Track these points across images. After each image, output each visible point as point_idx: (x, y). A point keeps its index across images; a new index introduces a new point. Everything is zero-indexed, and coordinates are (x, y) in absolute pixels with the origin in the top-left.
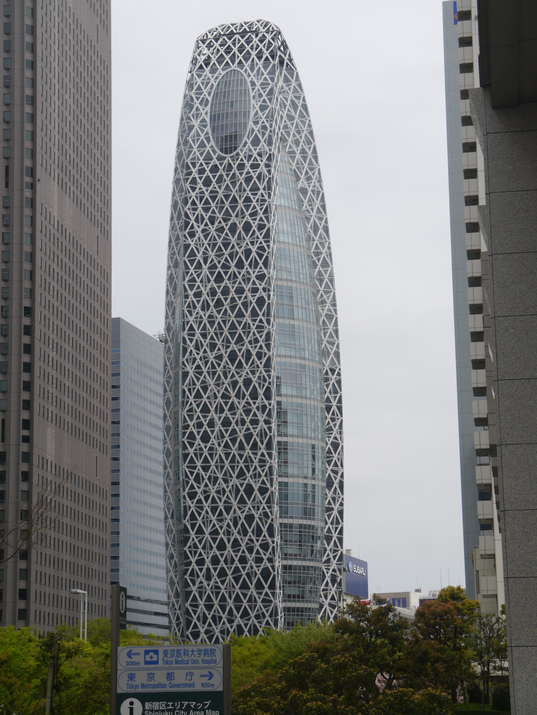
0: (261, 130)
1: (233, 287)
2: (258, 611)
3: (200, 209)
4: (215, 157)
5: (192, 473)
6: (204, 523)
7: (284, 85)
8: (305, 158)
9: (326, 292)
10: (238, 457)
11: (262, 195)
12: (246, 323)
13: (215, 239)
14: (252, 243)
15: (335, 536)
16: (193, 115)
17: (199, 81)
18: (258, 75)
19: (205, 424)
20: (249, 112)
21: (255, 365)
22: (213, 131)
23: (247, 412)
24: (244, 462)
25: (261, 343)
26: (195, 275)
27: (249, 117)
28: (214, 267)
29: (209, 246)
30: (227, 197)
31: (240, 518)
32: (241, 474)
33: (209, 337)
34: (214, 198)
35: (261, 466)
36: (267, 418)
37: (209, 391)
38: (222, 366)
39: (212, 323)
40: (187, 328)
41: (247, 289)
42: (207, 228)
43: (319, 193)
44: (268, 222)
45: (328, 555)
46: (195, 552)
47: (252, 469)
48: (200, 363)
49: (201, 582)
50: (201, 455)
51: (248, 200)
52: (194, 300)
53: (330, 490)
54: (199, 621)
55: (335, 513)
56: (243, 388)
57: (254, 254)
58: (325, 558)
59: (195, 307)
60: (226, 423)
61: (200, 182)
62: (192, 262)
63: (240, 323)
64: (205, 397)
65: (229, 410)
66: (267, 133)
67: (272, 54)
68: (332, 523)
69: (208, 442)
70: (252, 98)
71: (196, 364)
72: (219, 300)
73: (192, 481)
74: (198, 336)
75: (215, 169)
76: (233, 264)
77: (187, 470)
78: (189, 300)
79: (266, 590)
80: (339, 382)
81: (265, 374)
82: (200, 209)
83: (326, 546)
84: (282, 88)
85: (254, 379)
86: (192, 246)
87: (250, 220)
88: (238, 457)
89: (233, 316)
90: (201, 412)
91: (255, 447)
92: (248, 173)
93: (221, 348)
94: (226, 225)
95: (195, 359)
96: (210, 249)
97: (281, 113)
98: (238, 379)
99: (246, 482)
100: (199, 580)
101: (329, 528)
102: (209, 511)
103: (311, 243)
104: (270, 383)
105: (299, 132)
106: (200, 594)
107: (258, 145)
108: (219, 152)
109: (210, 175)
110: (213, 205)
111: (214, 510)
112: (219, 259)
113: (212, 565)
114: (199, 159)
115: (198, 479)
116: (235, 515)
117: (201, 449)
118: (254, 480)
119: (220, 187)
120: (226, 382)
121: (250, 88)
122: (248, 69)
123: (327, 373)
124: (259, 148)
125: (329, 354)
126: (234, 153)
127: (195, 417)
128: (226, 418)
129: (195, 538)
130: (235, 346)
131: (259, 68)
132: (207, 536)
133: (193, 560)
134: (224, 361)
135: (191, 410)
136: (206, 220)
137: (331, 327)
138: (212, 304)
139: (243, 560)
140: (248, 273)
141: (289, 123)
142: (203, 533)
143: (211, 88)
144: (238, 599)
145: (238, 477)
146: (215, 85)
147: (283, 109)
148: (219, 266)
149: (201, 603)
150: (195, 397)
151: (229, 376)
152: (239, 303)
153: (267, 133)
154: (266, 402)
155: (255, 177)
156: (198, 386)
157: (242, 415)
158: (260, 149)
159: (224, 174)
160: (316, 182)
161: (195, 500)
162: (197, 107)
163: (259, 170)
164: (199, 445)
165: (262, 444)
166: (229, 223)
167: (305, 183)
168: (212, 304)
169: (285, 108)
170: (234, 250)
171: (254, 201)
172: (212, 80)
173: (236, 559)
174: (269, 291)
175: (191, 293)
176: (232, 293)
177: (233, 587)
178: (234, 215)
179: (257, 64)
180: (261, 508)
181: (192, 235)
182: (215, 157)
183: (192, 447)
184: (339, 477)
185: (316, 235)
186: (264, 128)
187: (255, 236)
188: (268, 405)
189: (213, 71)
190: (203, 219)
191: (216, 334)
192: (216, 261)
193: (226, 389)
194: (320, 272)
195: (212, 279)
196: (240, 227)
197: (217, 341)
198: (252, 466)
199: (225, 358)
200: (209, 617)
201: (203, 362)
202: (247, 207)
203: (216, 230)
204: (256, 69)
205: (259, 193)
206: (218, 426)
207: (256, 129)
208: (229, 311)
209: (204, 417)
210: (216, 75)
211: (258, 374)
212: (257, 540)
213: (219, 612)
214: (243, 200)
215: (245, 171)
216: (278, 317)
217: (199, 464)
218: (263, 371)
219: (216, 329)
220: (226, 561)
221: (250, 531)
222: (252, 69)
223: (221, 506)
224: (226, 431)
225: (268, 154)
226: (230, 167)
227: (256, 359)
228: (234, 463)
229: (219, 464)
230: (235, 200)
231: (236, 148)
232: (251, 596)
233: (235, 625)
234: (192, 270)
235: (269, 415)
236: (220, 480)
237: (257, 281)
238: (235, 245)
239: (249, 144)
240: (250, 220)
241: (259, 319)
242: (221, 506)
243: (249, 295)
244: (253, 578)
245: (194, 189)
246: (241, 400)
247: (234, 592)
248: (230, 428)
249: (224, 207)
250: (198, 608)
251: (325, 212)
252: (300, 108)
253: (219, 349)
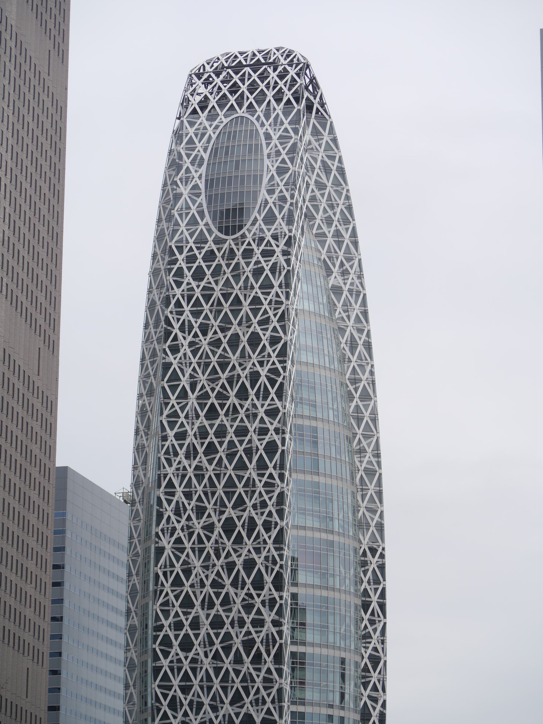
0: (278, 203)
1: (232, 426)
3: (187, 313)
4: (210, 239)
5: (165, 696)
7: (312, 139)
8: (339, 244)
9: (366, 437)
11: (277, 295)
12: (249, 479)
13: (208, 357)
14: (261, 363)
16: (181, 179)
17: (191, 131)
18: (275, 125)
19: (187, 624)
20: (261, 176)
21: (261, 539)
22: (209, 203)
23: (248, 608)
24: (241, 681)
25: (271, 507)
26: (177, 407)
27: (261, 183)
28: (206, 396)
29: (199, 366)
30: (226, 296)
32: (237, 699)
33: (195, 498)
34: (207, 298)
35: (266, 688)
36: (277, 618)
37: (193, 576)
38: (212, 540)
39: (200, 478)
40: (164, 484)
41: (251, 429)
42: (197, 340)
43: (358, 293)
44: (285, 333)
47: (252, 692)
48: (182, 535)
50: (180, 669)
51: (256, 301)
52: (176, 443)
56: (242, 573)
57: (263, 379)
59: (176, 454)
60: (217, 623)
61: (188, 275)
62: (173, 388)
63: (240, 478)
64: (187, 584)
65: (222, 605)
66: (287, 206)
67: (296, 95)
69: (190, 650)
70: (265, 157)
71: (175, 536)
72: (211, 444)
73: (165, 707)
74: (179, 495)
75: (210, 256)
76: (232, 394)
77: (158, 691)
78: (167, 444)
80: (382, 567)
81: (275, 554)
82: (187, 313)
84: (310, 143)
85: (260, 561)
86: (175, 365)
87: (258, 329)
89: (230, 468)
90: (181, 606)
91: (257, 659)
92: (258, 262)
93: (212, 514)
94: (225, 337)
95: (174, 529)
96: (199, 371)
97: (307, 178)
98: (236, 559)
99: (244, 711)
103: (346, 365)
104: (281, 567)
105: (332, 207)
107: (273, 223)
108: (216, 232)
109: (203, 265)
110: (206, 307)
112: (212, 385)
114: (188, 242)
115: (174, 705)
117: (179, 661)
118: (255, 708)
119: (216, 282)
120: (219, 563)
121: (264, 142)
122: (262, 115)
123: (364, 554)
124: (274, 227)
125: (368, 526)
126: (238, 235)
127: (172, 614)
128: (217, 617)
130: (232, 512)
131: (278, 115)
134: (216, 533)
135: (166, 603)
136: (196, 329)
137: (372, 488)
138: (201, 450)
140: (254, 406)
141: (317, 193)
143: (208, 141)
145: (232, 703)
146: (214, 137)
147: (310, 173)
148: (213, 395)
150: (172, 585)
151: (223, 555)
152: (241, 448)
153: (287, 206)
154: (276, 595)
155: (267, 269)
156: (178, 568)
157: (239, 612)
158: (276, 229)
159: (223, 263)
160: (355, 279)
162: (188, 168)
163: (273, 259)
164: (177, 654)
165: (269, 655)
166: (229, 334)
167: (340, 279)
168: (201, 450)
169: (313, 172)
170: (235, 373)
171: (265, 303)
172: (210, 131)
174: (284, 432)
175: (171, 434)
176: (231, 435)
178: (235, 322)
179: (275, 109)
181: (175, 349)
182: (210, 239)
183: (166, 657)
184: (379, 707)
185: (353, 355)
186: (283, 199)
187: (266, 353)
188: (278, 599)
189: (212, 117)
190: (191, 327)
191: (206, 494)
192: (208, 389)
193: (218, 574)
194: (357, 406)
195: (202, 414)
196: (244, 340)
197: (206, 504)
198: (253, 687)
199: (218, 529)
201: (186, 533)
202: (255, 312)
203: (209, 344)
204: (273, 116)
205: (273, 292)
206: (205, 628)
207: (270, 201)
208: (225, 461)
209: (185, 614)
210: (215, 123)
211: (264, 554)
214: (249, 301)
215: (254, 260)
216: (296, 471)
217: (176, 682)
218: (272, 549)
219: (205, 486)
222: (267, 116)
224: (217, 635)
225: (287, 237)
226: (232, 254)
227: (263, 531)
228: (227, 682)
229: (205, 684)
230: (237, 301)
231: (241, 227)
234: (173, 400)
235: (280, 613)
236: (206, 707)
237: (266, 419)
238: (237, 365)
239: (260, 221)
240: (258, 329)
241: (268, 473)
243: (255, 438)
245: (179, 284)
246: (239, 591)
248: (223, 632)
249: (222, 311)
251: (367, 321)
252: (334, 172)
253: (209, 516)
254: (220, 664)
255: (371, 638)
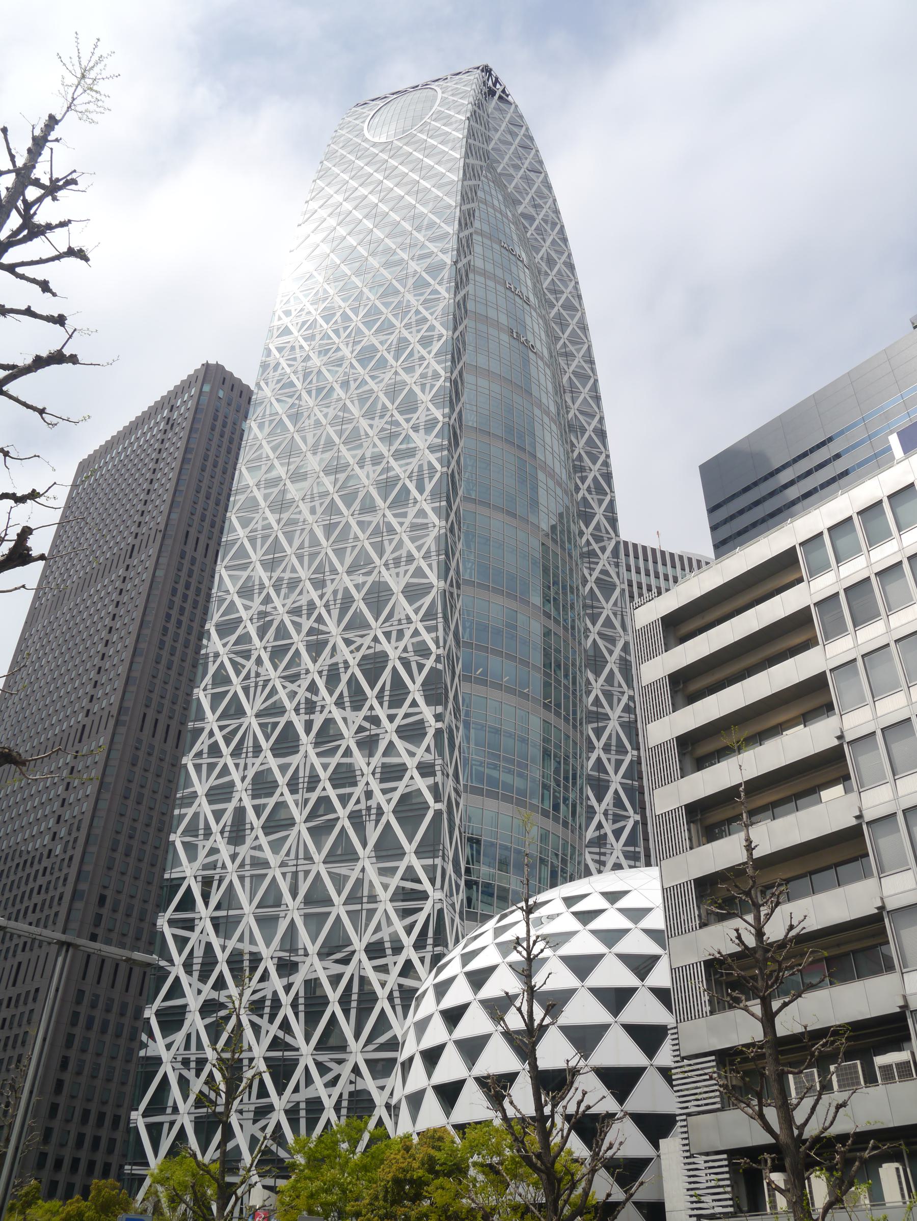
2: (378, 928)
6: (246, 690)
10: (355, 528)
15: (616, 781)
31: (347, 667)
35: (413, 540)
45: (600, 826)
46: (212, 767)
47: (389, 548)
49: (214, 851)
53: (597, 674)
54: (189, 972)
55: (613, 726)
58: (590, 833)
68: (607, 748)
79: (411, 859)
83: (593, 802)
88: (355, 528)
99: (370, 579)
100: (209, 844)
101: (599, 759)
102: (265, 657)
106: (207, 883)
111: (277, 654)
113: (254, 797)
116: (334, 660)
118: (394, 571)
125: (583, 430)
127: (264, 468)
129: (216, 731)
132: (251, 721)
133: (200, 787)
134: (346, 364)
137: (585, 392)
139: (344, 777)
142: (241, 712)
144: (317, 898)
149: (203, 912)
157: (375, 445)
161: (233, 638)
164: (265, 519)
173: (324, 775)
177: (309, 858)
180: (408, 633)
198: (391, 541)
200: (222, 957)
212: (391, 718)
213: (252, 941)
220: (293, 786)
221: (371, 694)
223: (299, 641)
232: (359, 883)
233: (298, 980)
242: (299, 641)
244: (370, 826)
247: (307, 873)
250: (192, 929)
254: (335, 519)
255: (597, 556)
